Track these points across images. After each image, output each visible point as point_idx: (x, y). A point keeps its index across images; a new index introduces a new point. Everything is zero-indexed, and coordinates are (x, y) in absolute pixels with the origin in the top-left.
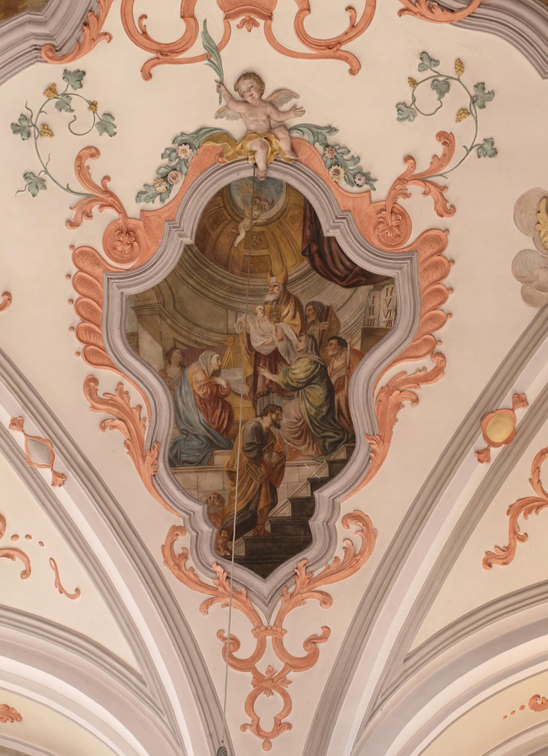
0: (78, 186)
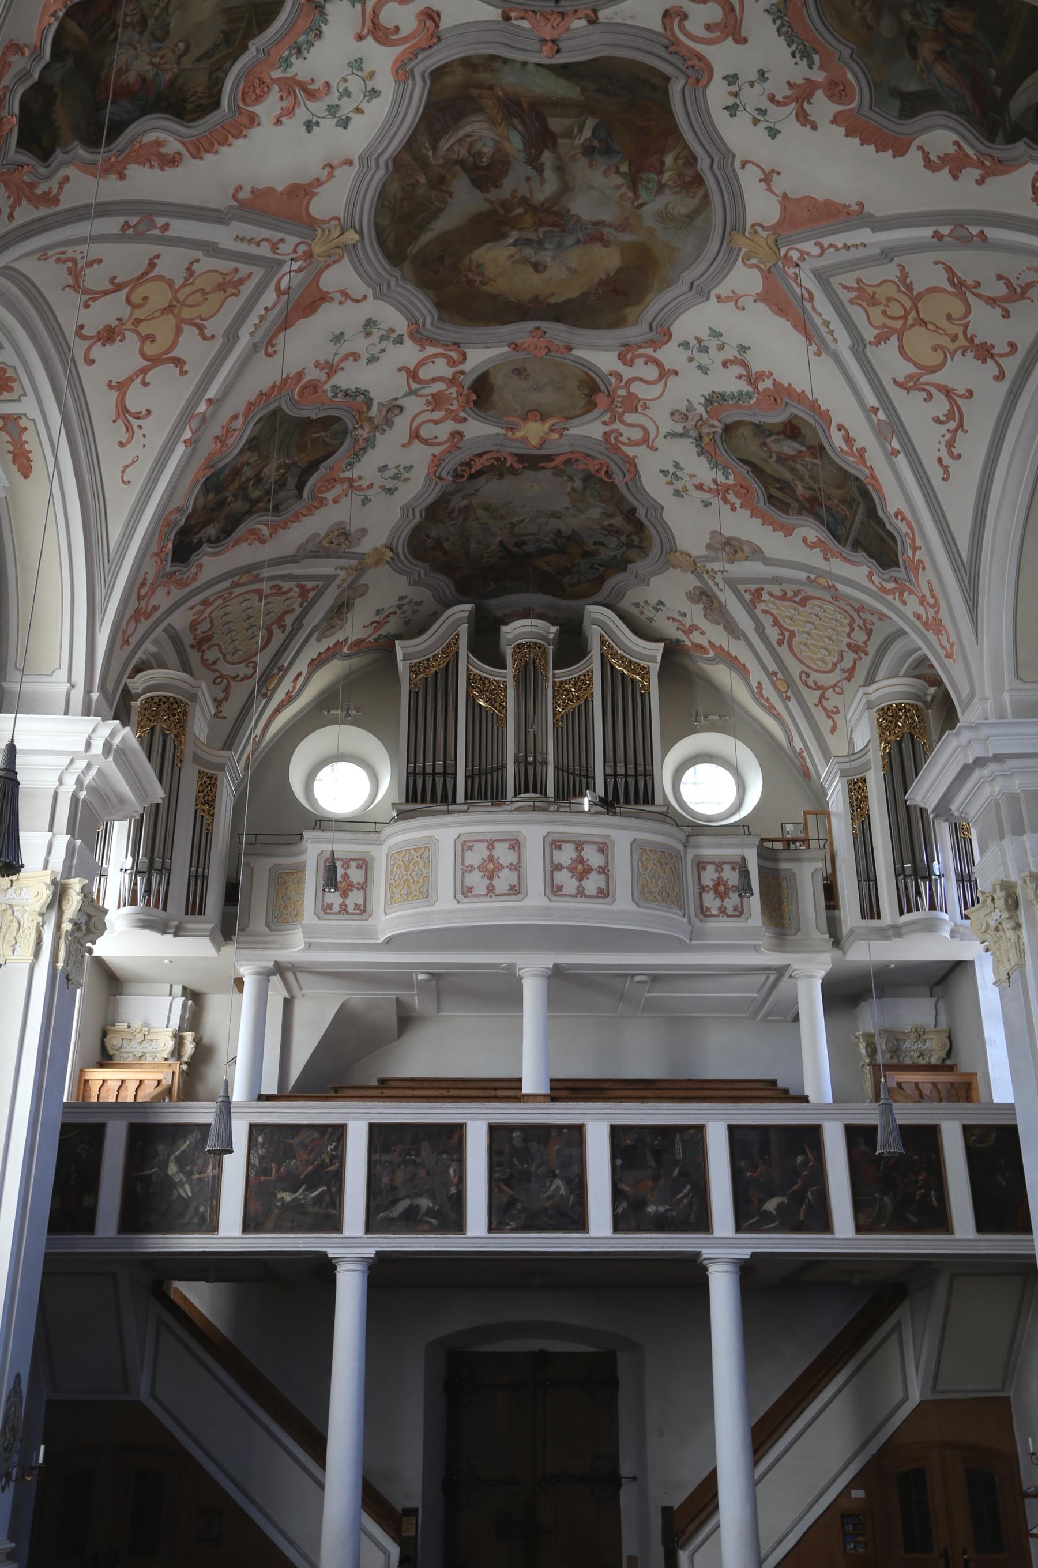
0: (337, 358)
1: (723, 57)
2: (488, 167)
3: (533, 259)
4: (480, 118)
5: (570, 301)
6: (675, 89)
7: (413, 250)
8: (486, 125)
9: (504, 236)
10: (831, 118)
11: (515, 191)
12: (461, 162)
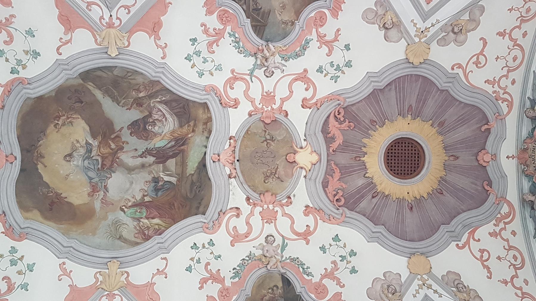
1: (221, 237)
2: (145, 129)
3: (75, 154)
4: (176, 125)
5: (41, 177)
6: (199, 218)
7: (90, 86)
8: (171, 129)
9: (94, 137)
11: (127, 143)
12: (150, 115)
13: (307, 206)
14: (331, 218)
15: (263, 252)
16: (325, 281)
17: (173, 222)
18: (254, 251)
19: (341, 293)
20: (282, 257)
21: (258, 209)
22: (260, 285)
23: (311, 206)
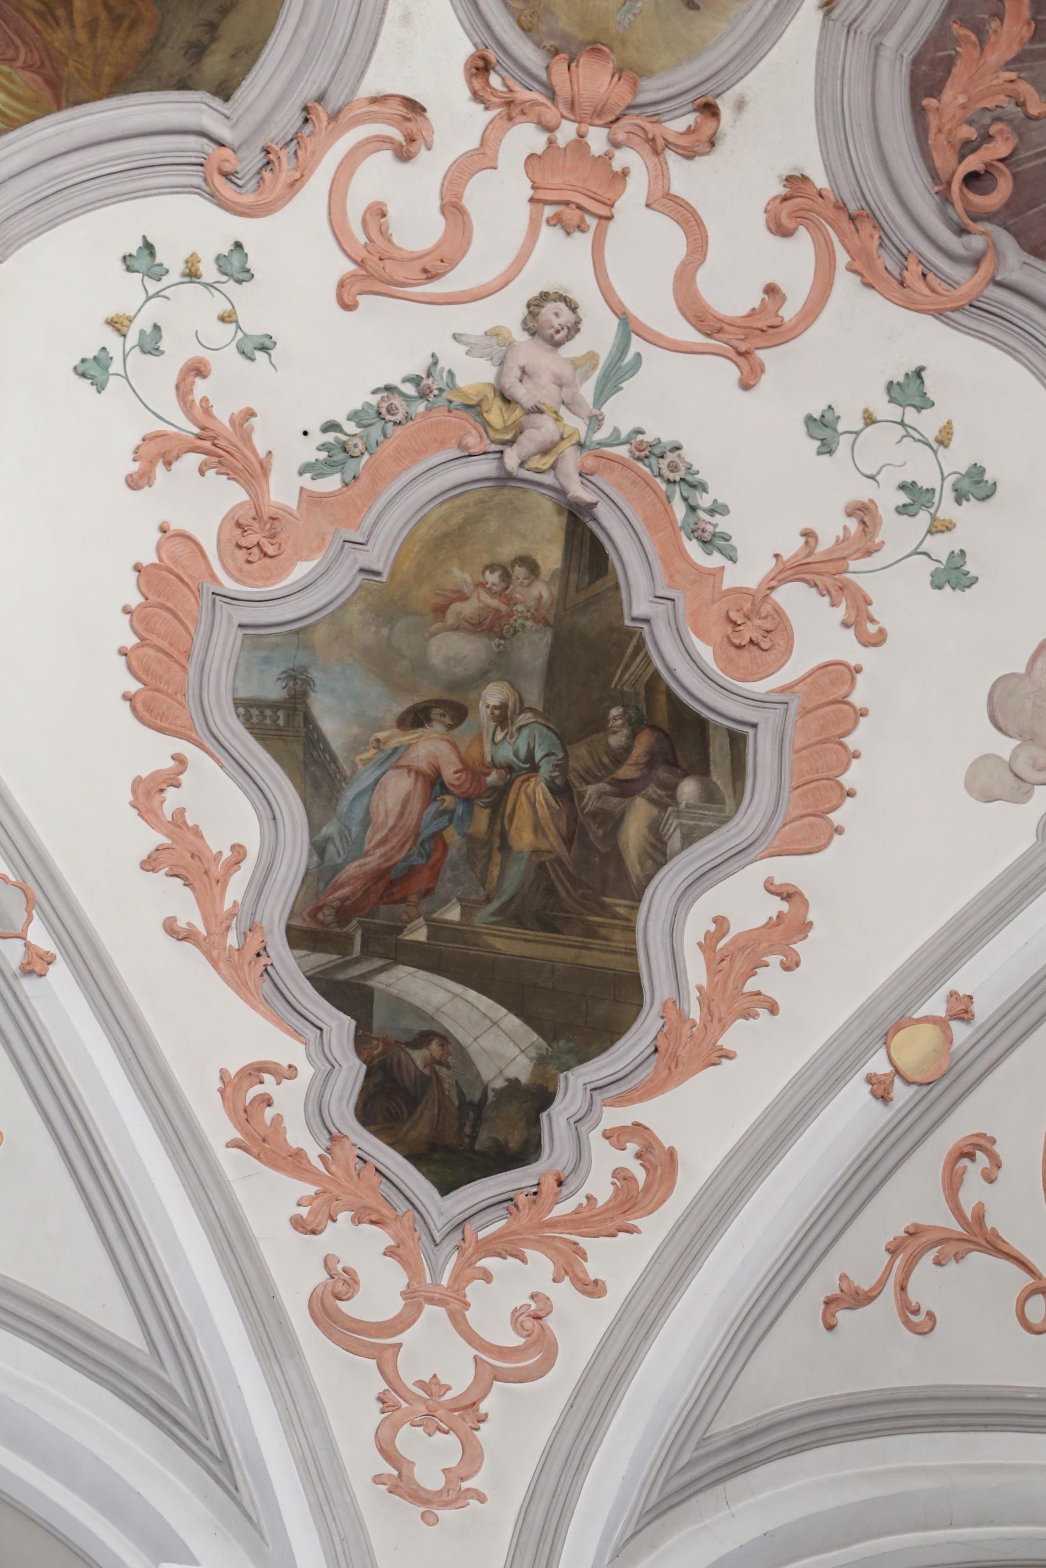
1: (296, 245)
6: (193, 108)
10: (175, 526)
13: (796, 182)
14: (912, 276)
15: (500, 376)
16: (795, 600)
17: (47, 94)
18: (453, 357)
19: (858, 670)
20: (596, 421)
21: (525, 139)
22: (445, 536)
23: (820, 181)
